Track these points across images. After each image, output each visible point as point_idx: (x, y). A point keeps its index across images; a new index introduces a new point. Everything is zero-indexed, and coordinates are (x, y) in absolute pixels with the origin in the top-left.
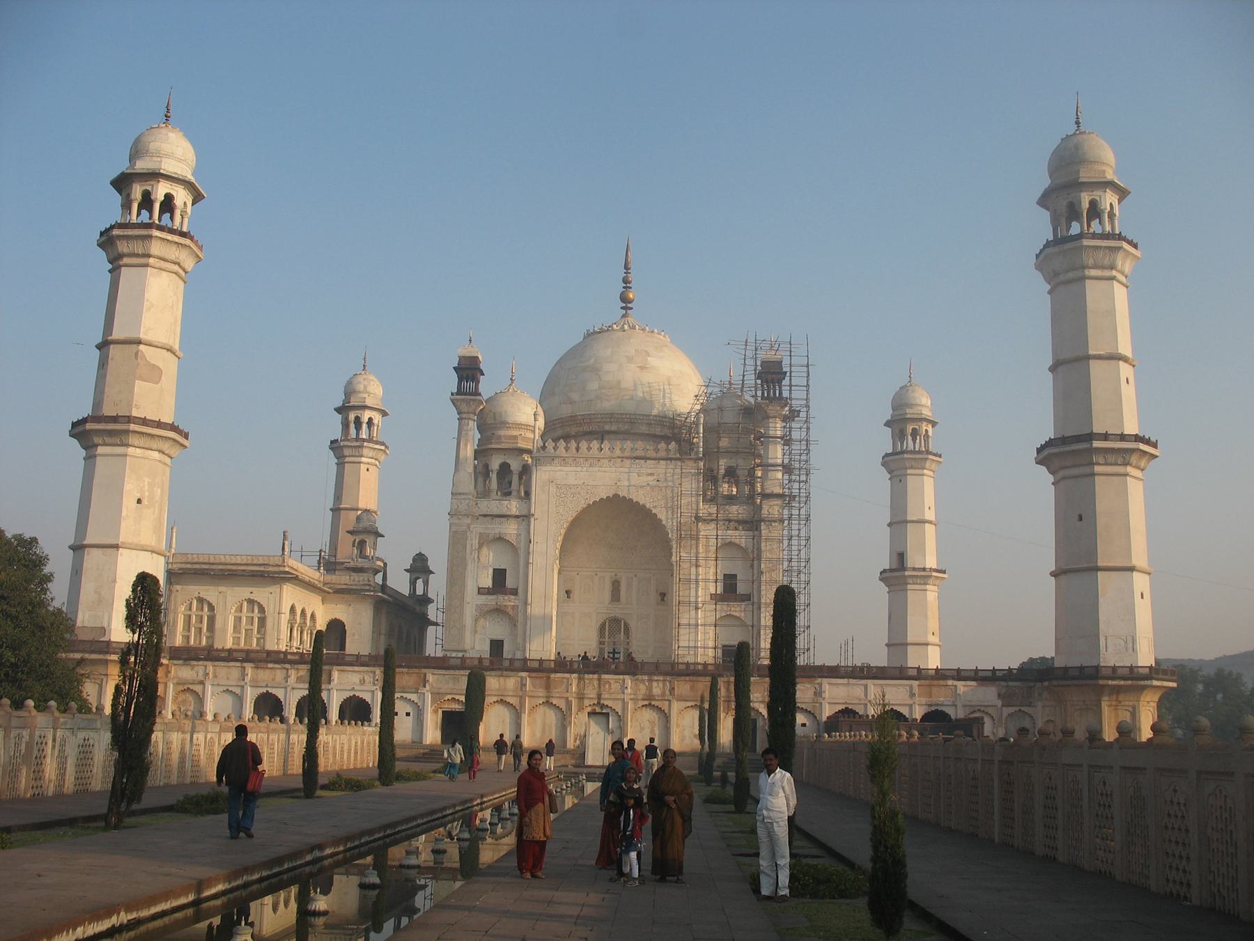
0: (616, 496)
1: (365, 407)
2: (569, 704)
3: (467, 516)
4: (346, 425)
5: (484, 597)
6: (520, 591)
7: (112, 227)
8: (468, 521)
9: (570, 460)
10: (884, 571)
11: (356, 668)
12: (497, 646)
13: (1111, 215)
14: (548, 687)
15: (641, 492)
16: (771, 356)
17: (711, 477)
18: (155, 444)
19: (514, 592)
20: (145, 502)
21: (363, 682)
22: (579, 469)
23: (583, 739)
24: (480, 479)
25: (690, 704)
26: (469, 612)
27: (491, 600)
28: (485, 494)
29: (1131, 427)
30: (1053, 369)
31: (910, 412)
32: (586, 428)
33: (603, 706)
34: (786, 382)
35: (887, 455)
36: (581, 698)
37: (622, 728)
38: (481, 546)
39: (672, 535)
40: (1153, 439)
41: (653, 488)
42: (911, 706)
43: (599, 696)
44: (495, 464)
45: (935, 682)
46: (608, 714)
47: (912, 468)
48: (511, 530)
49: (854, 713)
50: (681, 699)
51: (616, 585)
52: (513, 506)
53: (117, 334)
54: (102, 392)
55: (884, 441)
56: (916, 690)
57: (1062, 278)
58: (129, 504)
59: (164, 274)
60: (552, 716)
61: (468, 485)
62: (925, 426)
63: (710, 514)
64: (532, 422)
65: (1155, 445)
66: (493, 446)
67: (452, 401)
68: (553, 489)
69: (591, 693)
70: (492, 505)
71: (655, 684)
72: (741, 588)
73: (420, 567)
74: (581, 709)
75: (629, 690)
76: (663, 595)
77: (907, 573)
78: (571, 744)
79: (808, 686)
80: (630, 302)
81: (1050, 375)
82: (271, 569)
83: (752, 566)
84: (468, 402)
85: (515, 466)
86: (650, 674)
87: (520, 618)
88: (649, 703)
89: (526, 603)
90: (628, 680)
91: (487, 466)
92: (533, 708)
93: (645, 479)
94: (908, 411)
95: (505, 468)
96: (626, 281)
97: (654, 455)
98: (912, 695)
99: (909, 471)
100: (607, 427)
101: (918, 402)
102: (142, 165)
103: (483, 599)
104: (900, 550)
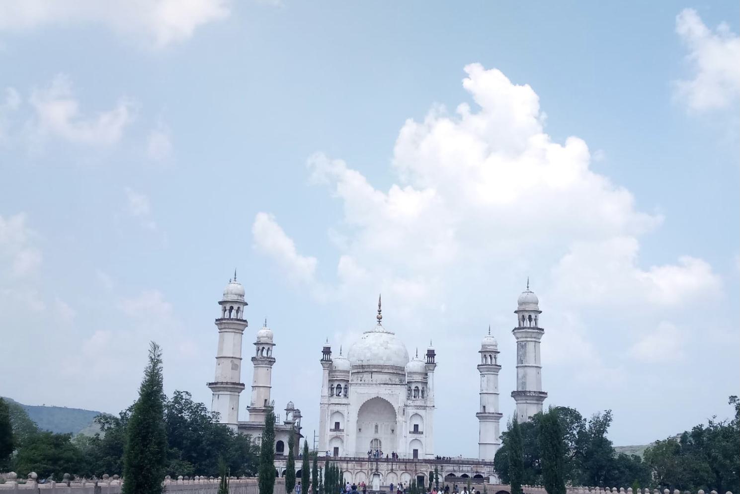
0: (378, 397)
5: (332, 432)
6: (345, 430)
7: (221, 319)
9: (362, 385)
10: (477, 413)
12: (336, 450)
14: (361, 466)
15: (387, 396)
17: (410, 390)
25: (404, 471)
27: (335, 434)
28: (332, 395)
30: (517, 367)
32: (366, 370)
39: (396, 411)
41: (390, 394)
43: (377, 470)
44: (335, 385)
45: (478, 466)
46: (379, 475)
49: (454, 475)
51: (377, 427)
52: (342, 400)
57: (520, 340)
59: (238, 334)
61: (326, 392)
70: (335, 400)
72: (420, 430)
73: (298, 415)
76: (393, 431)
80: (381, 318)
81: (516, 369)
85: (343, 385)
86: (392, 462)
91: (332, 385)
92: (357, 473)
93: (387, 392)
95: (339, 387)
96: (380, 311)
97: (390, 383)
100: (374, 370)
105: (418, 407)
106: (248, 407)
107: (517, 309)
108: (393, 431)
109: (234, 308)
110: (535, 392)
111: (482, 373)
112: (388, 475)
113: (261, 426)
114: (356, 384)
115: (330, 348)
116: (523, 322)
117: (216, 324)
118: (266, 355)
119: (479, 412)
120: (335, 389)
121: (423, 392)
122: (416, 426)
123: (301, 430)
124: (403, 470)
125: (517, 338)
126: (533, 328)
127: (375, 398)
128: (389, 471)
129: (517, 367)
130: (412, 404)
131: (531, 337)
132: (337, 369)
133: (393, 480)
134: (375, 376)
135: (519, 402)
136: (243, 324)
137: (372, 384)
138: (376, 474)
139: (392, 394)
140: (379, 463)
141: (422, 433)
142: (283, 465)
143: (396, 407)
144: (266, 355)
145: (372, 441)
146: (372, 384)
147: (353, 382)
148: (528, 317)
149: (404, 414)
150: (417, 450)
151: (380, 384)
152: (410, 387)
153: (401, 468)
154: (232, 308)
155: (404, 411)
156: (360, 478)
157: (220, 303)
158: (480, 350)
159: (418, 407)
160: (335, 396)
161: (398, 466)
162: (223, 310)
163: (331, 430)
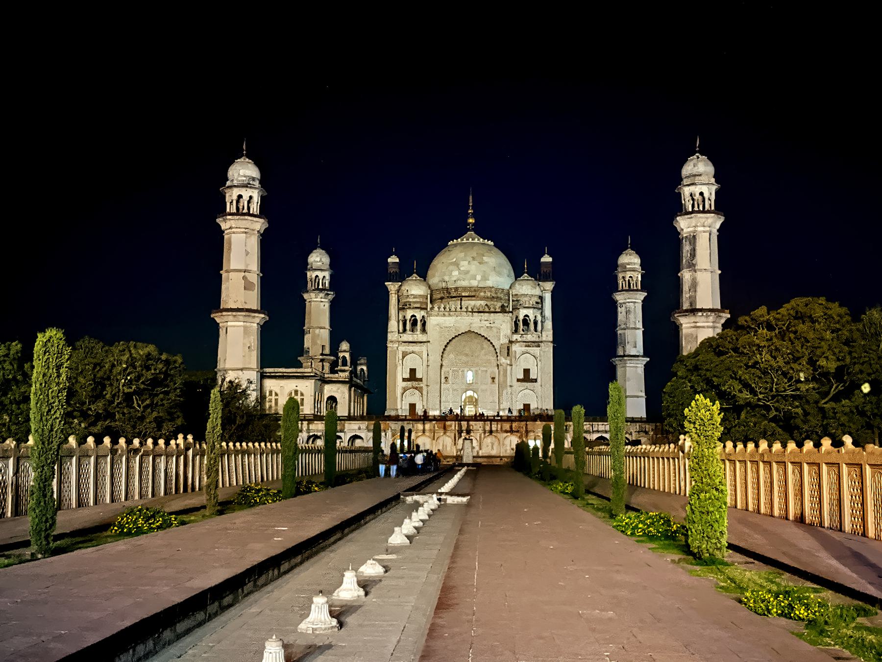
12: (413, 407)
38: (403, 357)
52: (419, 336)
68: (437, 328)
72: (532, 376)
76: (493, 378)
85: (419, 318)
87: (425, 393)
97: (487, 310)
103: (405, 384)
105: (528, 344)
121: (536, 323)
122: (527, 372)
124: (506, 432)
130: (520, 339)
132: (409, 293)
134: (465, 303)
141: (535, 381)
149: (508, 354)
150: (529, 405)
152: (517, 317)
155: (508, 350)
159: (528, 344)
160: (408, 332)
161: (499, 426)
163: (404, 380)
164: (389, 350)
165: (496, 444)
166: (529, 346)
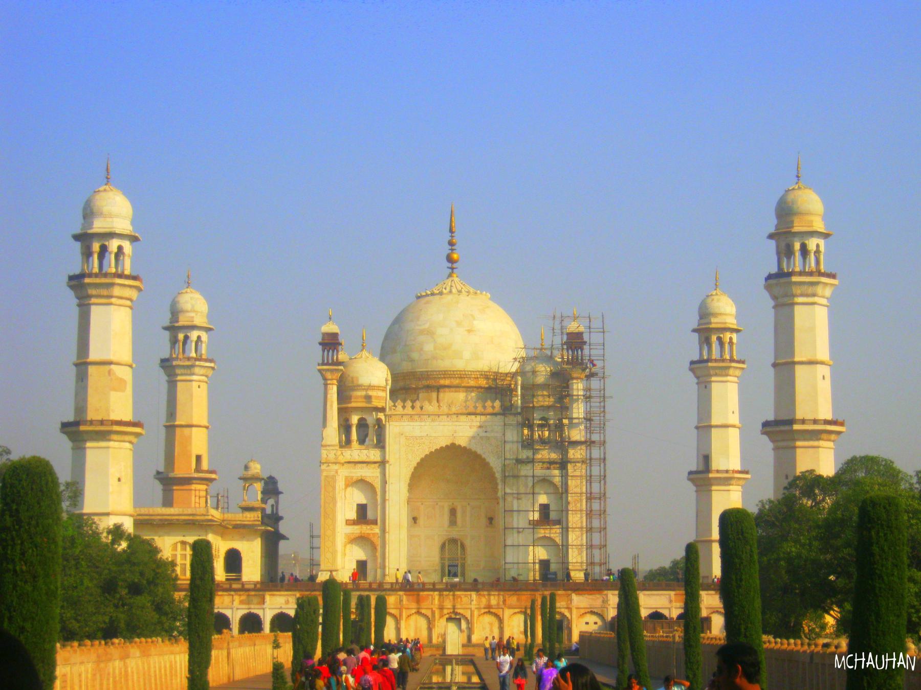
0: (453, 445)
1: (194, 327)
2: (433, 613)
3: (335, 463)
4: (174, 341)
8: (336, 467)
9: (416, 417)
10: (690, 473)
11: (282, 593)
13: (817, 252)
14: (418, 601)
16: (573, 327)
18: (127, 438)
19: (375, 522)
20: (123, 480)
21: (287, 602)
22: (423, 424)
23: (444, 636)
24: (342, 430)
25: (517, 610)
26: (340, 540)
27: (357, 530)
29: (825, 411)
30: (775, 365)
31: (715, 322)
32: (425, 383)
33: (456, 614)
34: (586, 347)
35: (692, 363)
36: (441, 608)
37: (470, 630)
39: (498, 475)
40: (840, 420)
41: (481, 438)
42: (669, 609)
43: (454, 608)
44: (355, 419)
46: (460, 619)
47: (716, 375)
48: (372, 474)
50: (510, 607)
51: (453, 512)
53: (93, 356)
54: (85, 400)
55: (692, 349)
56: (673, 597)
58: (113, 481)
59: (122, 308)
60: (423, 623)
62: (727, 336)
63: (528, 458)
64: (383, 383)
65: (842, 424)
66: (353, 405)
67: (320, 371)
69: (448, 604)
71: (492, 597)
72: (553, 516)
73: (271, 488)
74: (441, 616)
75: (474, 602)
76: (491, 520)
77: (711, 475)
78: (435, 641)
79: (598, 596)
80: (456, 261)
81: (772, 370)
82: (198, 518)
83: (561, 498)
84: (332, 371)
85: (371, 420)
88: (489, 610)
89: (384, 531)
90: (474, 594)
91: (347, 420)
94: (713, 320)
95: (362, 424)
98: (671, 601)
99: (713, 379)
100: (442, 382)
101: (722, 311)
102: (99, 226)
104: (706, 453)
106: (158, 473)
107: (772, 230)
108: (491, 520)
109: (110, 249)
110: (815, 422)
111: (701, 379)
112: (481, 618)
113: (183, 517)
114: (402, 415)
115: (335, 336)
116: (789, 258)
117: (71, 287)
118: (193, 355)
119: (694, 468)
120: (354, 430)
123: (281, 523)
125: (774, 298)
126: (811, 274)
127: (447, 446)
128: (483, 611)
129: (775, 365)
131: (807, 296)
133: (492, 631)
135: (781, 444)
136: (130, 286)
137: (439, 415)
138: (455, 618)
139: (488, 438)
140: (458, 593)
142: (241, 602)
143: (495, 464)
144: (193, 355)
145: (443, 546)
146: (439, 415)
147: (393, 412)
148: (797, 246)
151: (457, 414)
153: (508, 602)
154: (104, 250)
156: (416, 628)
157: (77, 238)
158: (695, 326)
160: (355, 444)
162: (83, 254)
163: (349, 523)
164: (325, 474)
165: (496, 624)
166: (548, 468)
